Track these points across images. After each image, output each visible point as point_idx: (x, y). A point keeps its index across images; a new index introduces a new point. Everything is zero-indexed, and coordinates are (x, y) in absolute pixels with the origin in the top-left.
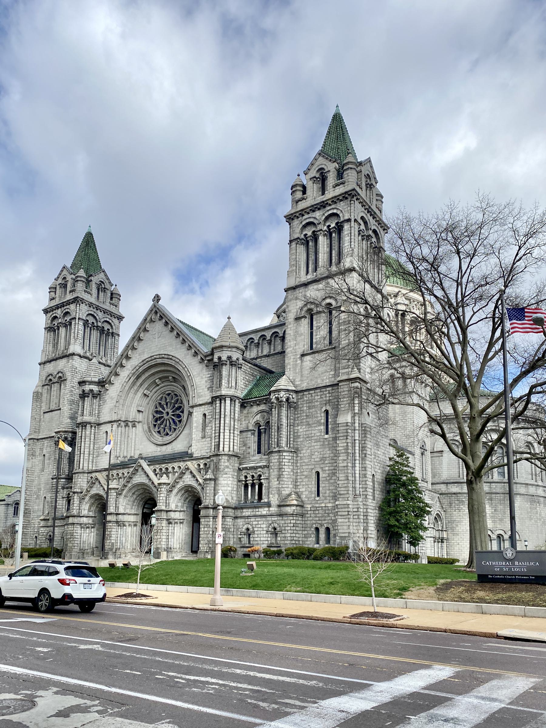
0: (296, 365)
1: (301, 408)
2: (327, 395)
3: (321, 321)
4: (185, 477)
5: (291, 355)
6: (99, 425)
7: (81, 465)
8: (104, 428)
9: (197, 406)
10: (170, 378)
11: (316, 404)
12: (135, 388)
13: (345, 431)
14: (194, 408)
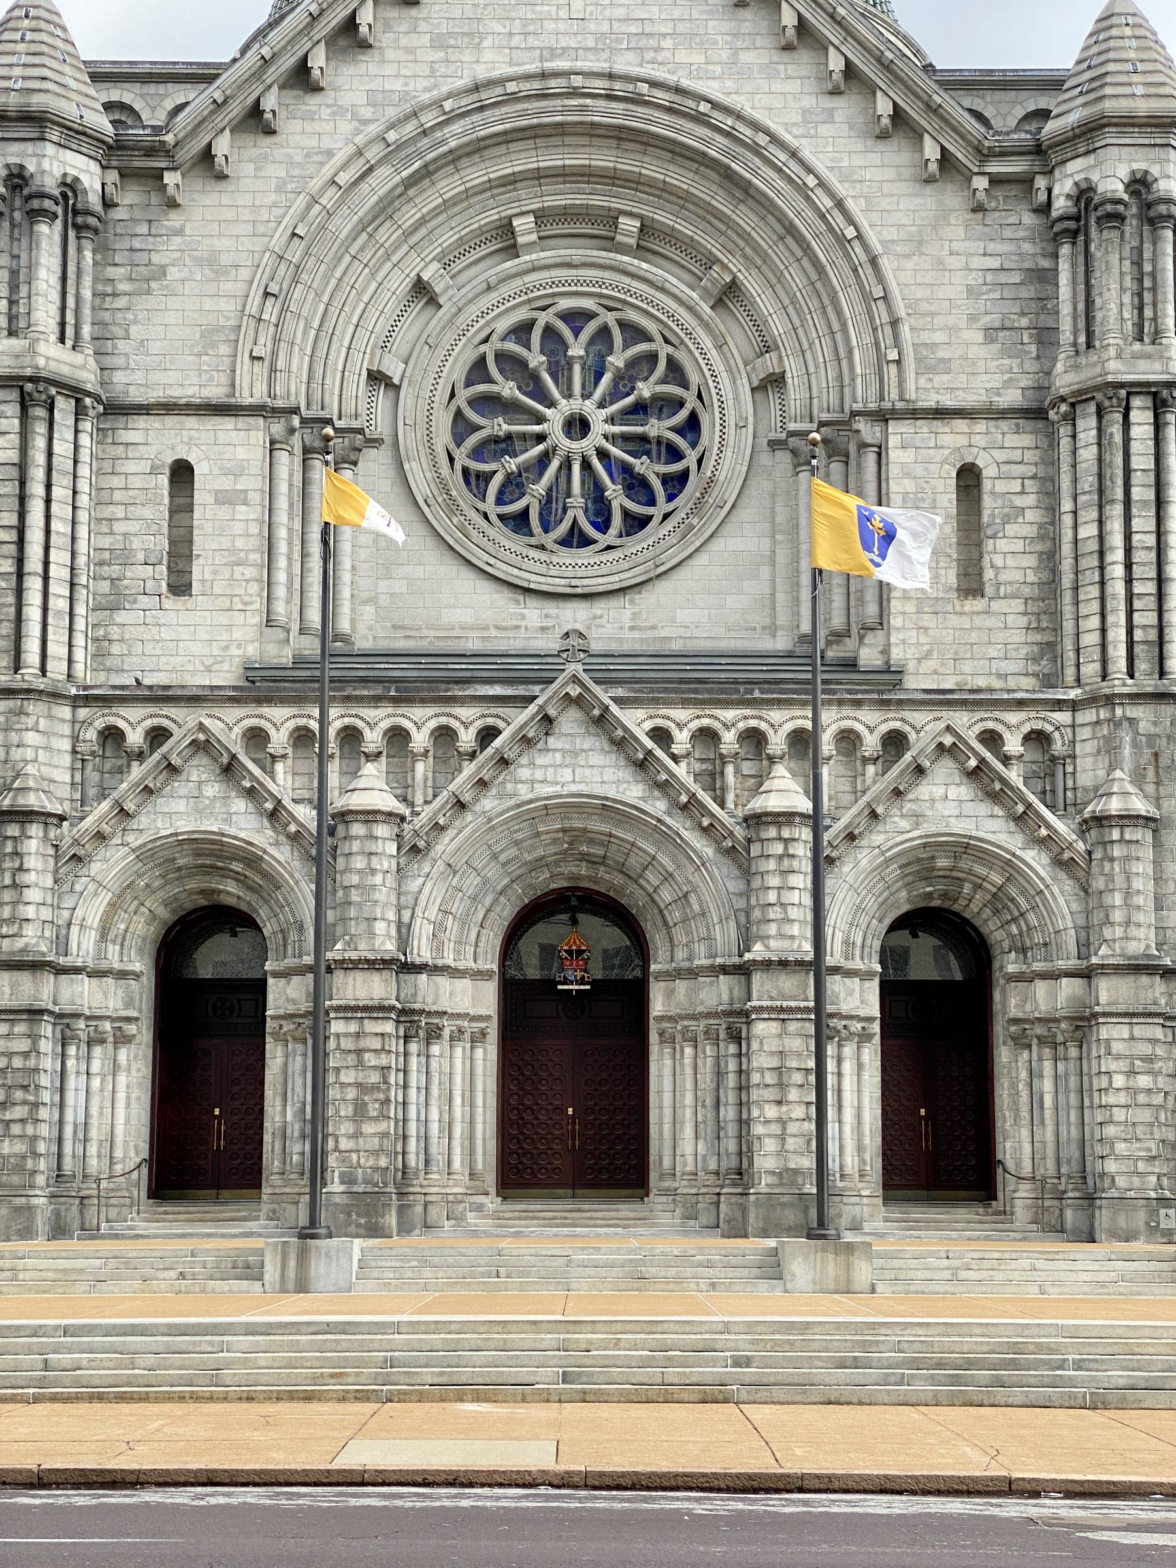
4: (926, 790)
6: (118, 410)
7: (32, 646)
8: (154, 443)
9: (915, 414)
10: (629, 225)
12: (387, 234)
14: (897, 432)
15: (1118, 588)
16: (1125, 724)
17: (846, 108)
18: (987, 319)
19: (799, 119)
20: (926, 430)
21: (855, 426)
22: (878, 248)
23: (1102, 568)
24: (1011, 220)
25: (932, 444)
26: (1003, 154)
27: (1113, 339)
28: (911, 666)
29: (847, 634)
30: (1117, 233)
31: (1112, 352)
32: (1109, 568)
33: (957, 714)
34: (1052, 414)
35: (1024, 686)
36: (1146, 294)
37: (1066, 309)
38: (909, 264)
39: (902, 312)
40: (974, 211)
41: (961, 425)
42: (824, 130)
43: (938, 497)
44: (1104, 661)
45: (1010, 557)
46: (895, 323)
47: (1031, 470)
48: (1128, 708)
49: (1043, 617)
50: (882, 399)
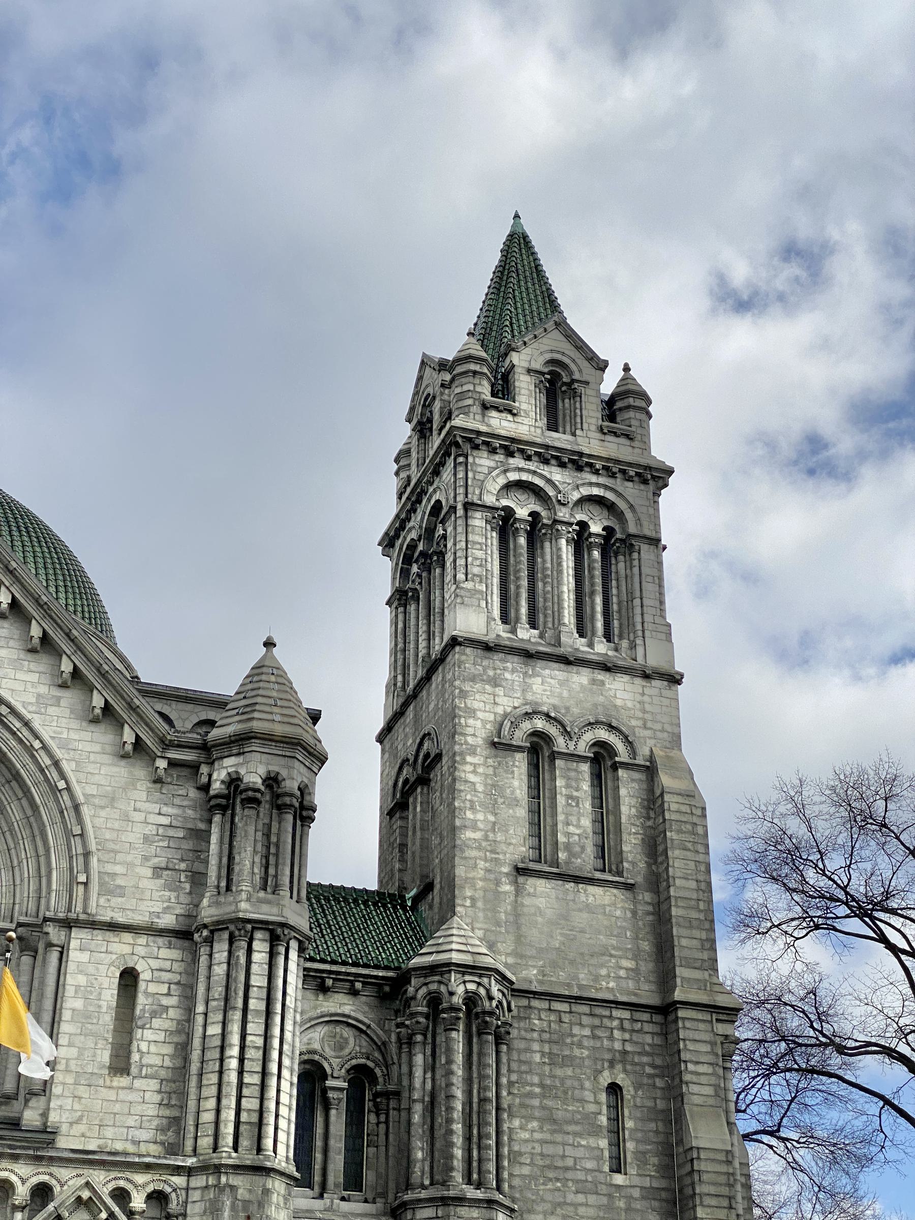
0: (497, 893)
1: (519, 1051)
2: (617, 1034)
3: (573, 787)
5: (474, 853)
9: (93, 925)
11: (577, 1052)
13: (722, 1179)
14: (78, 937)
15: (232, 1077)
16: (228, 1190)
17: (70, 698)
18: (156, 860)
19: (34, 700)
20: (100, 938)
21: (46, 929)
22: (81, 799)
23: (222, 1060)
24: (180, 792)
25: (104, 949)
26: (180, 746)
27: (245, 887)
28: (64, 1128)
29: (15, 1097)
30: (255, 812)
31: (244, 896)
32: (227, 1060)
33: (96, 1173)
34: (196, 936)
35: (152, 1152)
36: (271, 857)
37: (213, 861)
38: (103, 813)
39: (93, 847)
40: (155, 782)
41: (127, 937)
42: (52, 710)
43: (104, 992)
44: (216, 1136)
45: (152, 1045)
46: (87, 855)
47: (177, 978)
48: (231, 1177)
49: (173, 1096)
50: (69, 910)
